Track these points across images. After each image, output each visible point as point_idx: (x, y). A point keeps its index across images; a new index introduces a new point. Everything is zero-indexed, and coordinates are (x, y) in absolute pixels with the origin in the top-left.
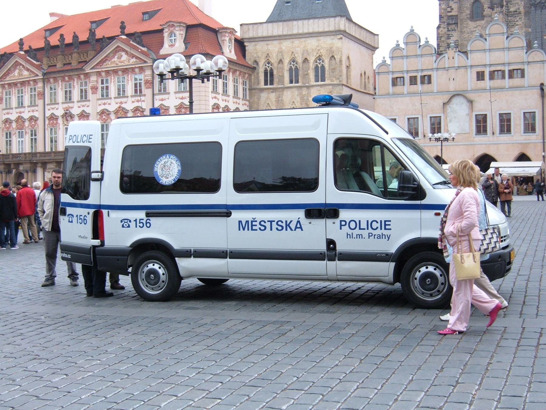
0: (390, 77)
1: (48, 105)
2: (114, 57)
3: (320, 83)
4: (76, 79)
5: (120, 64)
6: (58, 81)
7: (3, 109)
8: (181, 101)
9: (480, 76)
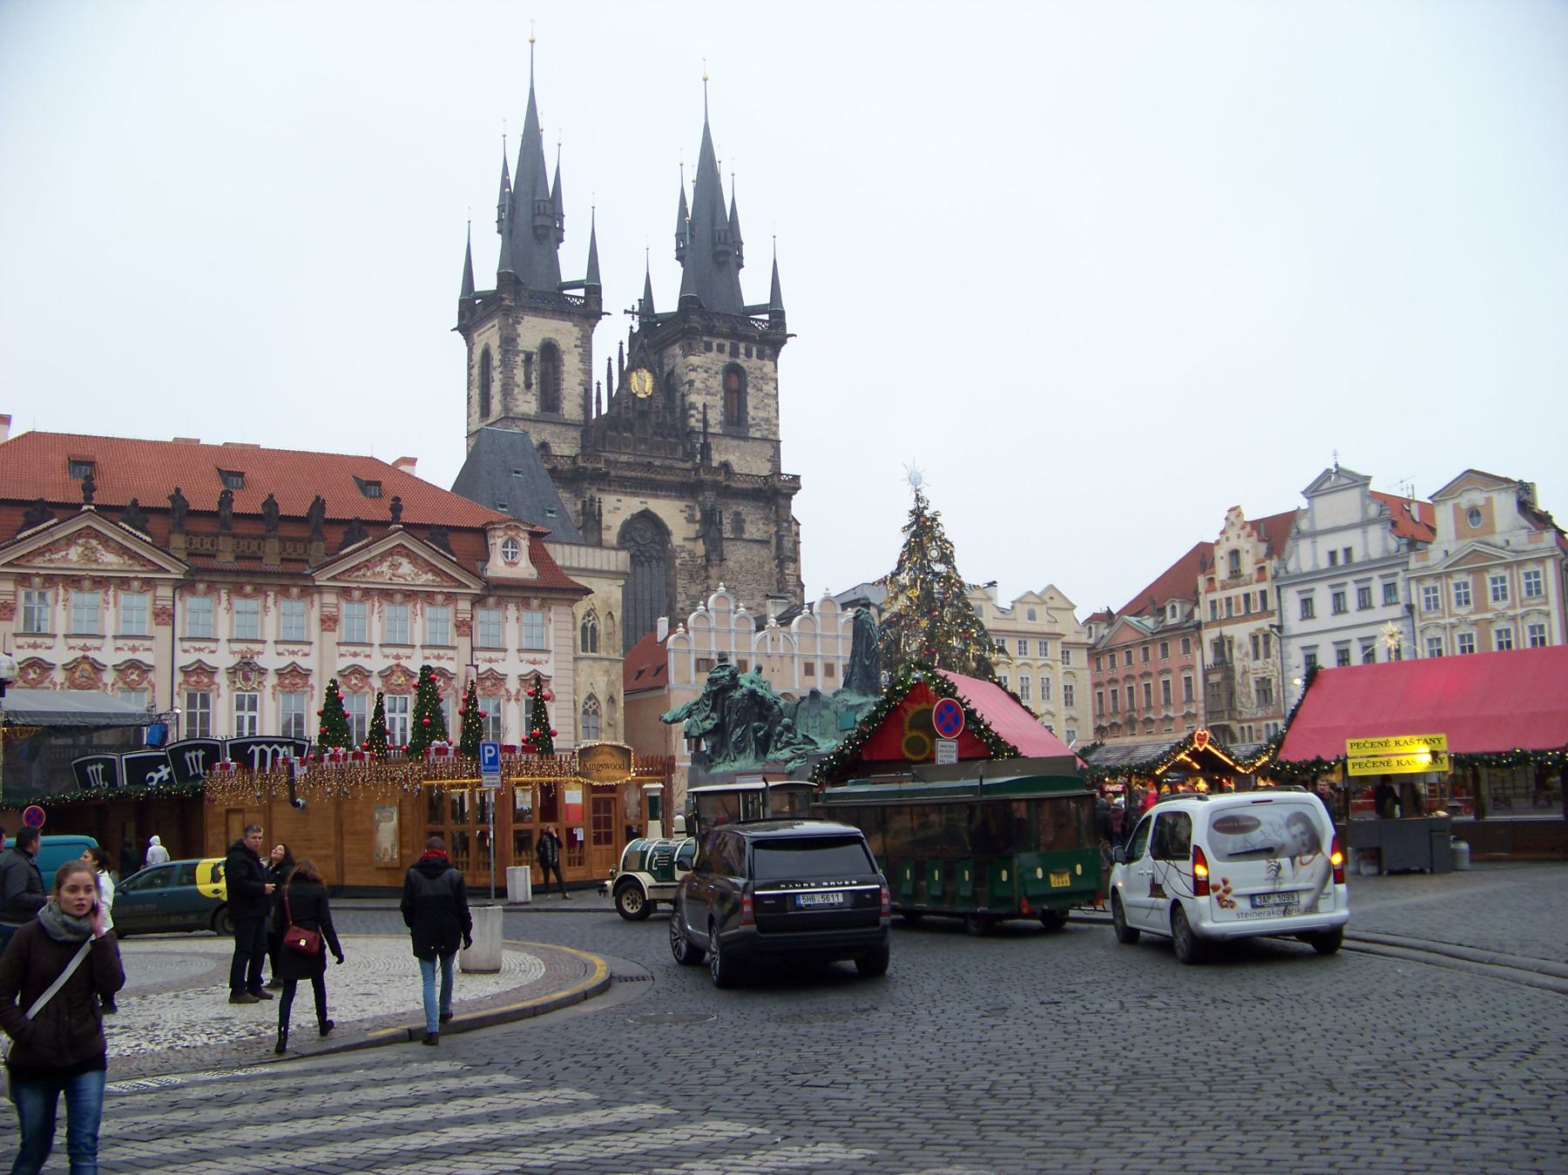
0: (693, 658)
1: (182, 639)
2: (381, 562)
3: (591, 654)
4: (272, 595)
5: (396, 580)
6: (218, 591)
7: (15, 635)
8: (532, 667)
9: (809, 669)
